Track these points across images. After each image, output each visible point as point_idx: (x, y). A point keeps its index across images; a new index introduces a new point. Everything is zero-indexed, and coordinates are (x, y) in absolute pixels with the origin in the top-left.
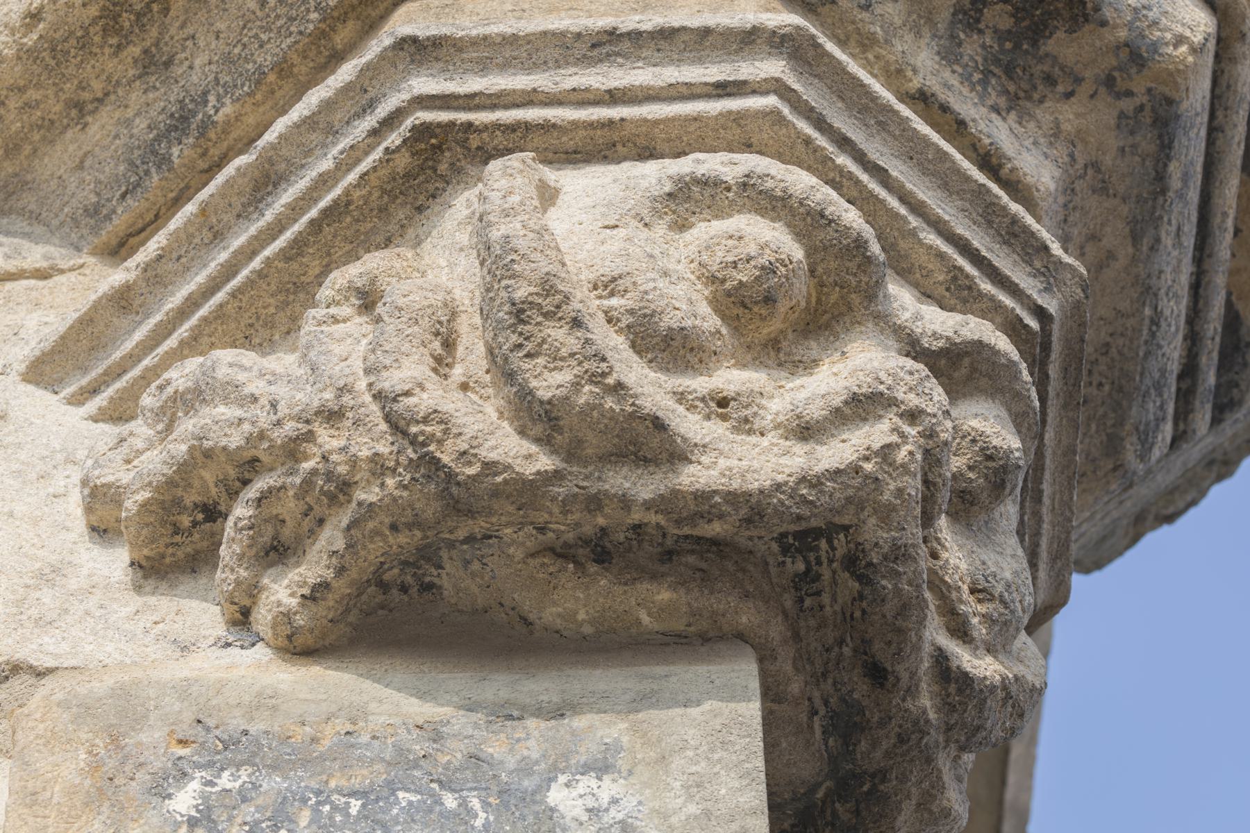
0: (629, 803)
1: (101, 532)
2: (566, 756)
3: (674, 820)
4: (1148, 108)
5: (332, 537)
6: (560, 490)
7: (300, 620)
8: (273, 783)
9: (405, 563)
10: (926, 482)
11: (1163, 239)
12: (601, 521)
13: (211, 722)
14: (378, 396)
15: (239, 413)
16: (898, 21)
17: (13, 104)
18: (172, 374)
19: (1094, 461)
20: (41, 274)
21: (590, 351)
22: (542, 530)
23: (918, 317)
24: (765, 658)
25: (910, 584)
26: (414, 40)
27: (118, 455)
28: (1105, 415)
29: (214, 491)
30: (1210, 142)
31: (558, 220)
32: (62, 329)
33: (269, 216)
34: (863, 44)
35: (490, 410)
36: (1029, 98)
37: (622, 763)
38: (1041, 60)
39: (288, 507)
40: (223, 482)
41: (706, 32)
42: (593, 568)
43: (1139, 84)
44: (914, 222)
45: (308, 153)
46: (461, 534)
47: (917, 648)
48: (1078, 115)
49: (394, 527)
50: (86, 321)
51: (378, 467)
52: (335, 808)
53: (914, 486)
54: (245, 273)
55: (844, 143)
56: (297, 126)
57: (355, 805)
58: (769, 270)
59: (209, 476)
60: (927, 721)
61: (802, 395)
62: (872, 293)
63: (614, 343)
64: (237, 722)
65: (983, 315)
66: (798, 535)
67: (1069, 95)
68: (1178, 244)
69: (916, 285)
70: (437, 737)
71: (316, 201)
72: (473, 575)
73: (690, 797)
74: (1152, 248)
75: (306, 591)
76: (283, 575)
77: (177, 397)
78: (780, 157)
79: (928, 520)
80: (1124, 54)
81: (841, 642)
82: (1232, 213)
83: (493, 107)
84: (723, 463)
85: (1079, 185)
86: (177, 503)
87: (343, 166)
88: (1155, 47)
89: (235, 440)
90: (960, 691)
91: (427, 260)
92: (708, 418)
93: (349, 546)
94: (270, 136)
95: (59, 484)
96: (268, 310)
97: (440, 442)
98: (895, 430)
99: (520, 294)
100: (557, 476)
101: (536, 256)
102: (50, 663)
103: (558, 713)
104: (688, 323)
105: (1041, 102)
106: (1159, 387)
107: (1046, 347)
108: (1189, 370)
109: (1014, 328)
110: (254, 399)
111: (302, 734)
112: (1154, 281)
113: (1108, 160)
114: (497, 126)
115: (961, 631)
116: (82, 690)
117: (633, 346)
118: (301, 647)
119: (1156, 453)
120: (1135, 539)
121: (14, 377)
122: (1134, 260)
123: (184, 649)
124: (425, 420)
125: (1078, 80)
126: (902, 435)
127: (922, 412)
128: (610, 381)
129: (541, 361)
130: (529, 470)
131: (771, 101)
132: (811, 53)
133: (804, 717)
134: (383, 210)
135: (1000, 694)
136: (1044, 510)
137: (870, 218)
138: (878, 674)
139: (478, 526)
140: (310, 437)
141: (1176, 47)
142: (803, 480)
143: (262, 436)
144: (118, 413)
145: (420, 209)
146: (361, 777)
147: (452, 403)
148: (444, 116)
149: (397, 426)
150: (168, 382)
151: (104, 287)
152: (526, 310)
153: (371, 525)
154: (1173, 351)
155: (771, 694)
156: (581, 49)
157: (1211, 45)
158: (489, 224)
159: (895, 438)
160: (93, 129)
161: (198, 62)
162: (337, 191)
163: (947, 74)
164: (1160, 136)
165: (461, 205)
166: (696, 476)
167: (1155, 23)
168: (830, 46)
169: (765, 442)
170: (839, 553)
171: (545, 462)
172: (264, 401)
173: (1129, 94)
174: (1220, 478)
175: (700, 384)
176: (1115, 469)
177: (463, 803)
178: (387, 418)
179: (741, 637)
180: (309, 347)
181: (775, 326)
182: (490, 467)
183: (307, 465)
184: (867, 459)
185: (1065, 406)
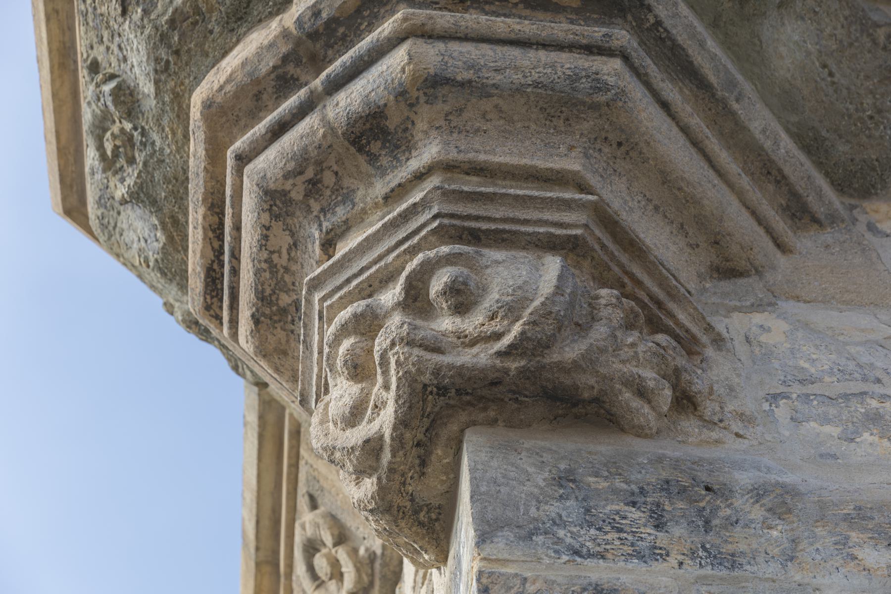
4: (426, 91)
6: (384, 481)
11: (494, 81)
16: (364, 192)
19: (600, 115)
24: (474, 423)
25: (450, 371)
28: (578, 110)
36: (410, 141)
38: (396, 132)
43: (415, 94)
44: (382, 263)
48: (422, 121)
55: (348, 281)
60: (523, 367)
67: (413, 123)
74: (497, 88)
80: (400, 98)
88: (401, 84)
90: (516, 349)
92: (379, 415)
98: (394, 355)
100: (379, 479)
105: (413, 136)
112: (514, 87)
113: (447, 108)
115: (498, 336)
117: (353, 427)
122: (500, 96)
125: (408, 118)
126: (397, 353)
127: (393, 340)
130: (375, 488)
132: (316, 281)
141: (404, 73)
142: (396, 401)
156: (307, 352)
163: (388, 178)
164: (441, 85)
173: (417, 98)
176: (608, 105)
179: (462, 431)
184: (398, 372)
185: (492, 200)
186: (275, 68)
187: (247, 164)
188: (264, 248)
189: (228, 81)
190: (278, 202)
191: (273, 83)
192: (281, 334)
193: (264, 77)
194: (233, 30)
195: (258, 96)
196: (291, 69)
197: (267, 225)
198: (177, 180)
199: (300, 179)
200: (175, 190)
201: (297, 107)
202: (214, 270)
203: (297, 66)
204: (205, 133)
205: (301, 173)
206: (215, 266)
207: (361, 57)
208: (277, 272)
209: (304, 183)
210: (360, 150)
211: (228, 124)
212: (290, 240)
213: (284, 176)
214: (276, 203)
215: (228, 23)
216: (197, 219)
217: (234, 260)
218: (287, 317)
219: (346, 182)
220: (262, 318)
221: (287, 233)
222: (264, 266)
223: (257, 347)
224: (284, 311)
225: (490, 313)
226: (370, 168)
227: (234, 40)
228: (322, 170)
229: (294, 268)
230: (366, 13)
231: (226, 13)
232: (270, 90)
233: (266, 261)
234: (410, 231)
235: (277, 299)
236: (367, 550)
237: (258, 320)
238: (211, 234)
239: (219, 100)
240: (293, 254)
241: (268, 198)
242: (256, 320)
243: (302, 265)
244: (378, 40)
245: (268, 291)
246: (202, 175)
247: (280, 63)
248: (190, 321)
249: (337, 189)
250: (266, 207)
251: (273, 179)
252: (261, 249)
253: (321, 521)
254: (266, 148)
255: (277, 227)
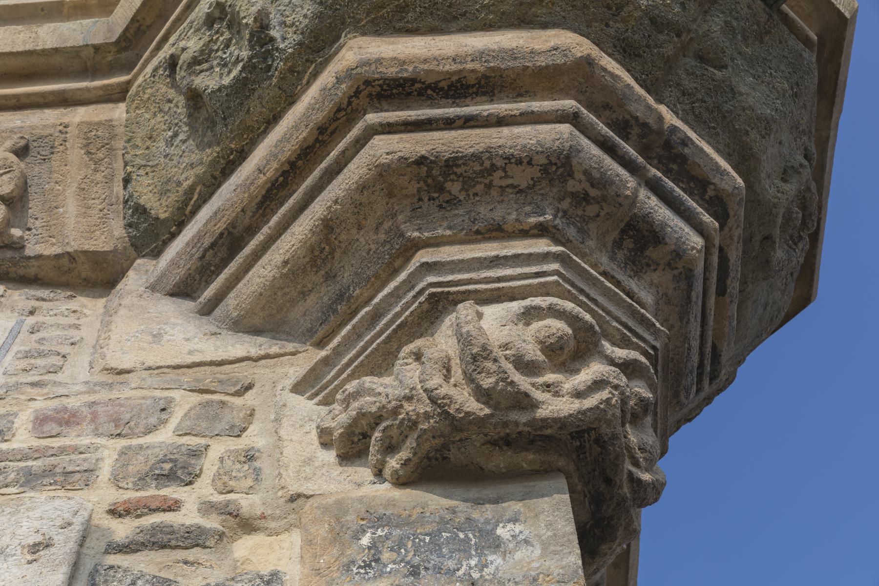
0: (526, 533)
1: (325, 445)
2: (501, 517)
3: (543, 538)
5: (411, 443)
7: (401, 473)
8: (397, 532)
9: (437, 450)
10: (622, 411)
12: (508, 431)
13: (372, 512)
14: (425, 391)
15: (374, 399)
17: (279, 294)
18: (347, 387)
20: (293, 354)
21: (501, 370)
22: (486, 435)
23: (613, 352)
26: (427, 263)
27: (330, 417)
29: (366, 428)
30: (705, 284)
31: (485, 324)
32: (304, 373)
33: (378, 328)
34: (583, 256)
35: (465, 393)
37: (522, 518)
39: (395, 432)
40: (369, 424)
41: (530, 255)
42: (505, 448)
43: (680, 265)
44: (608, 318)
45: (391, 305)
46: (457, 438)
47: (622, 471)
49: (434, 437)
50: (313, 370)
51: (427, 416)
52: (420, 540)
53: (618, 412)
54: (370, 349)
55: (582, 291)
56: (386, 296)
57: (427, 539)
58: (561, 338)
59: (364, 423)
61: (576, 382)
62: (597, 344)
63: (509, 367)
64: (381, 511)
65: (634, 349)
66: (577, 432)
67: (655, 270)
68: (696, 321)
69: (609, 341)
70: (454, 512)
71: (395, 322)
72: (462, 453)
73: (548, 529)
75: (402, 462)
76: (394, 457)
77: (349, 395)
78: (559, 297)
79: (623, 425)
80: (674, 254)
81: (594, 470)
82: (713, 309)
83: (457, 285)
84: (550, 408)
85: (660, 302)
86: (353, 433)
87: (404, 309)
88: (684, 251)
89: (374, 409)
90: (638, 486)
91: (437, 341)
92: (543, 392)
93: (418, 445)
94: (377, 300)
95: (307, 428)
96: (382, 362)
97: (449, 406)
98: (610, 393)
99: (474, 351)
100: (492, 415)
101: (479, 337)
102: (311, 493)
103: (496, 501)
104: (534, 358)
105: (646, 272)
106: (691, 372)
107: (657, 360)
108: (701, 365)
109: (645, 353)
110: (380, 394)
111: (405, 514)
114: (458, 292)
115: (636, 464)
116: (324, 502)
118: (401, 482)
119: (692, 396)
120: (678, 428)
121: (287, 391)
123: (359, 485)
124: (443, 398)
125: (658, 265)
126: (613, 394)
128: (509, 380)
129: (483, 375)
130: (482, 414)
131: (555, 278)
133: (582, 498)
134: (419, 324)
135: (652, 486)
136: (658, 419)
137: (593, 317)
138: (609, 481)
139: (463, 435)
140: (401, 406)
142: (579, 412)
143: (384, 407)
144: (326, 402)
145: (432, 323)
146: (428, 528)
147: (452, 392)
148: (440, 290)
149: (433, 400)
150: (346, 390)
151: (319, 357)
152: (477, 356)
153: (425, 437)
154: (695, 359)
155: (572, 491)
156: (487, 263)
157: (704, 250)
158: (461, 327)
159: (610, 396)
160: (309, 301)
161: (345, 275)
162: (403, 318)
163: (612, 265)
165: (449, 321)
166: (542, 413)
167: (684, 243)
168: (574, 257)
169: (564, 399)
170: (592, 438)
171: (487, 411)
172: (383, 394)
174: (707, 405)
175: (540, 380)
177: (466, 536)
178: (429, 398)
179: (559, 470)
180: (398, 374)
181: (564, 357)
182: (468, 414)
183: (401, 417)
184: (601, 403)
186: (636, 118)
187: (571, 124)
188: (507, 161)
189: (612, 75)
190: (561, 170)
191: (621, 118)
192: (413, 188)
193: (626, 110)
194: (615, 47)
195: (607, 106)
196: (636, 131)
197: (533, 162)
198: (449, 7)
199: (587, 185)
200: (439, 6)
201: (630, 157)
202: (413, 85)
203: (639, 135)
204: (565, 64)
205: (592, 185)
206: (417, 86)
207: (682, 203)
208: (483, 176)
209: (584, 189)
210: (623, 232)
211: (577, 84)
212: (524, 185)
213: (586, 170)
214: (557, 166)
215: (619, 40)
216: (466, 62)
217: (461, 122)
218: (435, 192)
219: (592, 226)
220: (426, 168)
221: (531, 183)
222: (487, 164)
223: (389, 165)
224: (441, 189)
225: (642, 447)
226: (610, 245)
227: (610, 51)
228: (598, 203)
229: (494, 192)
230: (692, 185)
231: (628, 38)
232: (614, 116)
233: (493, 165)
234: (637, 330)
235: (453, 181)
236: (22, 238)
237: (422, 163)
238: (454, 78)
239: (597, 72)
240: (508, 190)
241: (564, 161)
242: (421, 161)
243: (502, 201)
244: (698, 213)
245: (459, 171)
246: (517, 64)
247: (641, 121)
248: (262, 20)
249: (585, 220)
250: (554, 160)
251: (580, 161)
252: (505, 158)
253: (17, 173)
254: (589, 138)
255: (535, 172)
